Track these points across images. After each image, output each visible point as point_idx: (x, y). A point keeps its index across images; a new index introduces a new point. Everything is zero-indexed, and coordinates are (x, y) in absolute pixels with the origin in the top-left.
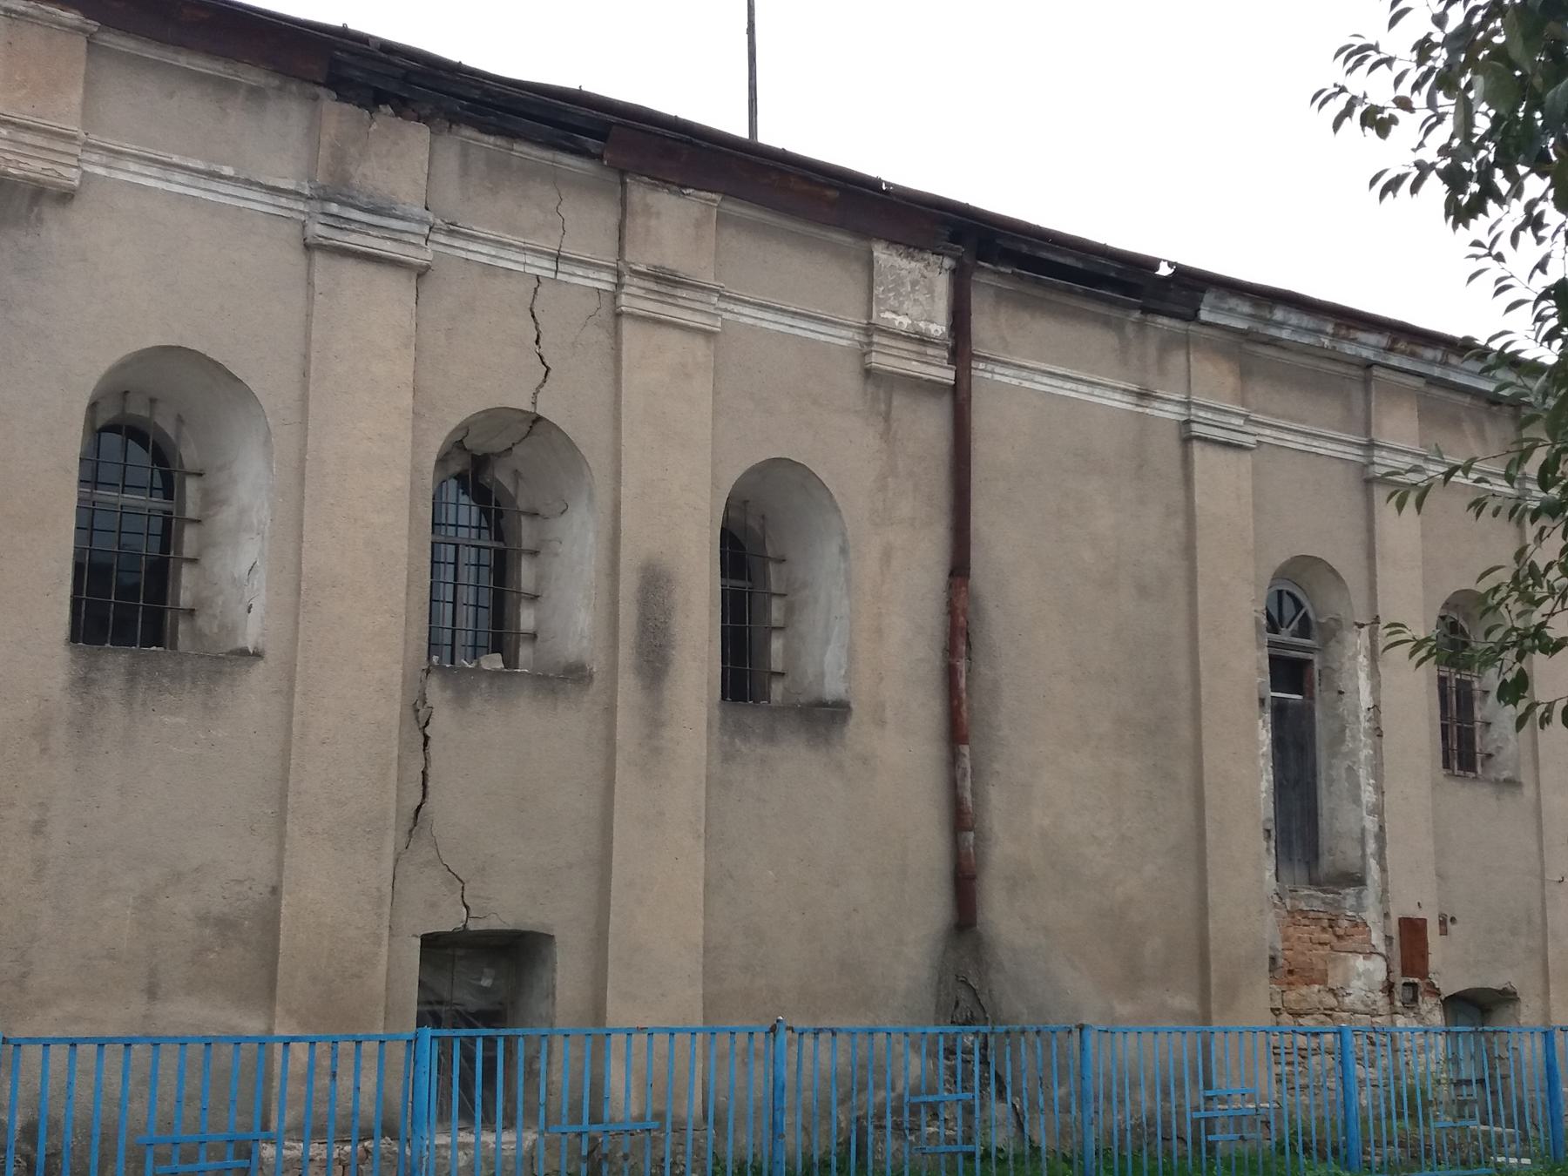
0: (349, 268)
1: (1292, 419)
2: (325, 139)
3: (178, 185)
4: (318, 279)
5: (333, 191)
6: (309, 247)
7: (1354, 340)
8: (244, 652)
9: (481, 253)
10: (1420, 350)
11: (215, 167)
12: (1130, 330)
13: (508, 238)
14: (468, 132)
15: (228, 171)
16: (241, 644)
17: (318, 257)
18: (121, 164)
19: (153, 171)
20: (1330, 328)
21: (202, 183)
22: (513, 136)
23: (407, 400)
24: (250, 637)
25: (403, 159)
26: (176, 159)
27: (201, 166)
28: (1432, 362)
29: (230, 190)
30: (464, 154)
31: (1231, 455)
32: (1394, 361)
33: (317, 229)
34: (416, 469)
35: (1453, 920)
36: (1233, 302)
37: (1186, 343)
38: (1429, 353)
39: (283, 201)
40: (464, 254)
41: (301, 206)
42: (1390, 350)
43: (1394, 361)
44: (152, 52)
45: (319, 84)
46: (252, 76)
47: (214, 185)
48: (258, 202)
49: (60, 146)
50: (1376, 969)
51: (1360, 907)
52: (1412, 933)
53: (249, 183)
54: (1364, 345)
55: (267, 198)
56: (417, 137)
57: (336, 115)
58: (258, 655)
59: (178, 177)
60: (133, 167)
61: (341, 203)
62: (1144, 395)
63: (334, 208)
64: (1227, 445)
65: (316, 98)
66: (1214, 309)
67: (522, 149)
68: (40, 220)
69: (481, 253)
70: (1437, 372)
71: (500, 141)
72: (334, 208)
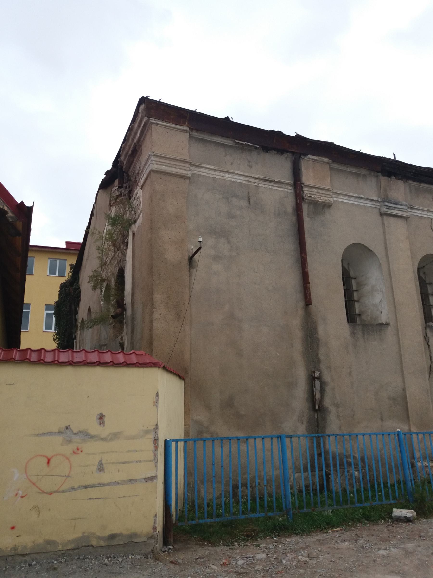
0: (392, 220)
2: (382, 186)
3: (352, 201)
4: (386, 223)
5: (386, 199)
6: (381, 215)
8: (382, 324)
9: (418, 213)
11: (360, 196)
13: (424, 209)
14: (411, 182)
15: (363, 196)
16: (380, 322)
17: (385, 217)
18: (339, 197)
19: (346, 198)
21: (357, 200)
22: (420, 181)
23: (409, 253)
24: (383, 319)
25: (399, 190)
26: (351, 194)
27: (356, 195)
29: (363, 201)
30: (410, 188)
33: (384, 210)
34: (414, 272)
39: (374, 203)
40: (413, 214)
41: (378, 204)
44: (342, 168)
45: (378, 172)
46: (364, 172)
47: (359, 201)
48: (369, 204)
49: (328, 193)
53: (367, 199)
55: (371, 203)
56: (401, 184)
57: (384, 180)
58: (387, 324)
59: (352, 199)
60: (342, 197)
61: (388, 202)
63: (387, 204)
65: (377, 176)
67: (423, 185)
68: (324, 213)
69: (418, 213)
71: (418, 184)
72: (387, 204)
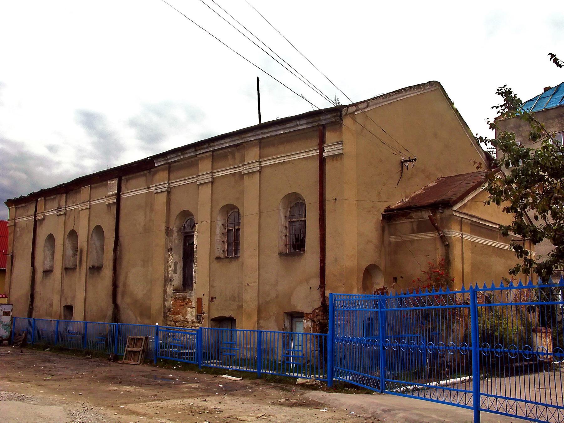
1: (182, 177)
7: (187, 153)
10: (202, 147)
12: (148, 174)
20: (180, 154)
28: (207, 148)
31: (162, 194)
32: (199, 152)
35: (215, 298)
36: (159, 160)
37: (155, 173)
38: (205, 146)
42: (196, 151)
43: (199, 152)
50: (194, 312)
51: (191, 296)
52: (200, 301)
54: (190, 153)
62: (149, 188)
64: (161, 192)
66: (157, 162)
70: (211, 149)
